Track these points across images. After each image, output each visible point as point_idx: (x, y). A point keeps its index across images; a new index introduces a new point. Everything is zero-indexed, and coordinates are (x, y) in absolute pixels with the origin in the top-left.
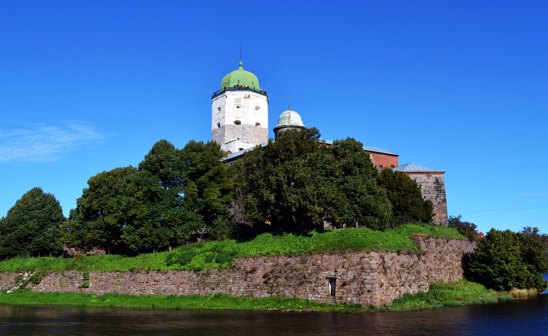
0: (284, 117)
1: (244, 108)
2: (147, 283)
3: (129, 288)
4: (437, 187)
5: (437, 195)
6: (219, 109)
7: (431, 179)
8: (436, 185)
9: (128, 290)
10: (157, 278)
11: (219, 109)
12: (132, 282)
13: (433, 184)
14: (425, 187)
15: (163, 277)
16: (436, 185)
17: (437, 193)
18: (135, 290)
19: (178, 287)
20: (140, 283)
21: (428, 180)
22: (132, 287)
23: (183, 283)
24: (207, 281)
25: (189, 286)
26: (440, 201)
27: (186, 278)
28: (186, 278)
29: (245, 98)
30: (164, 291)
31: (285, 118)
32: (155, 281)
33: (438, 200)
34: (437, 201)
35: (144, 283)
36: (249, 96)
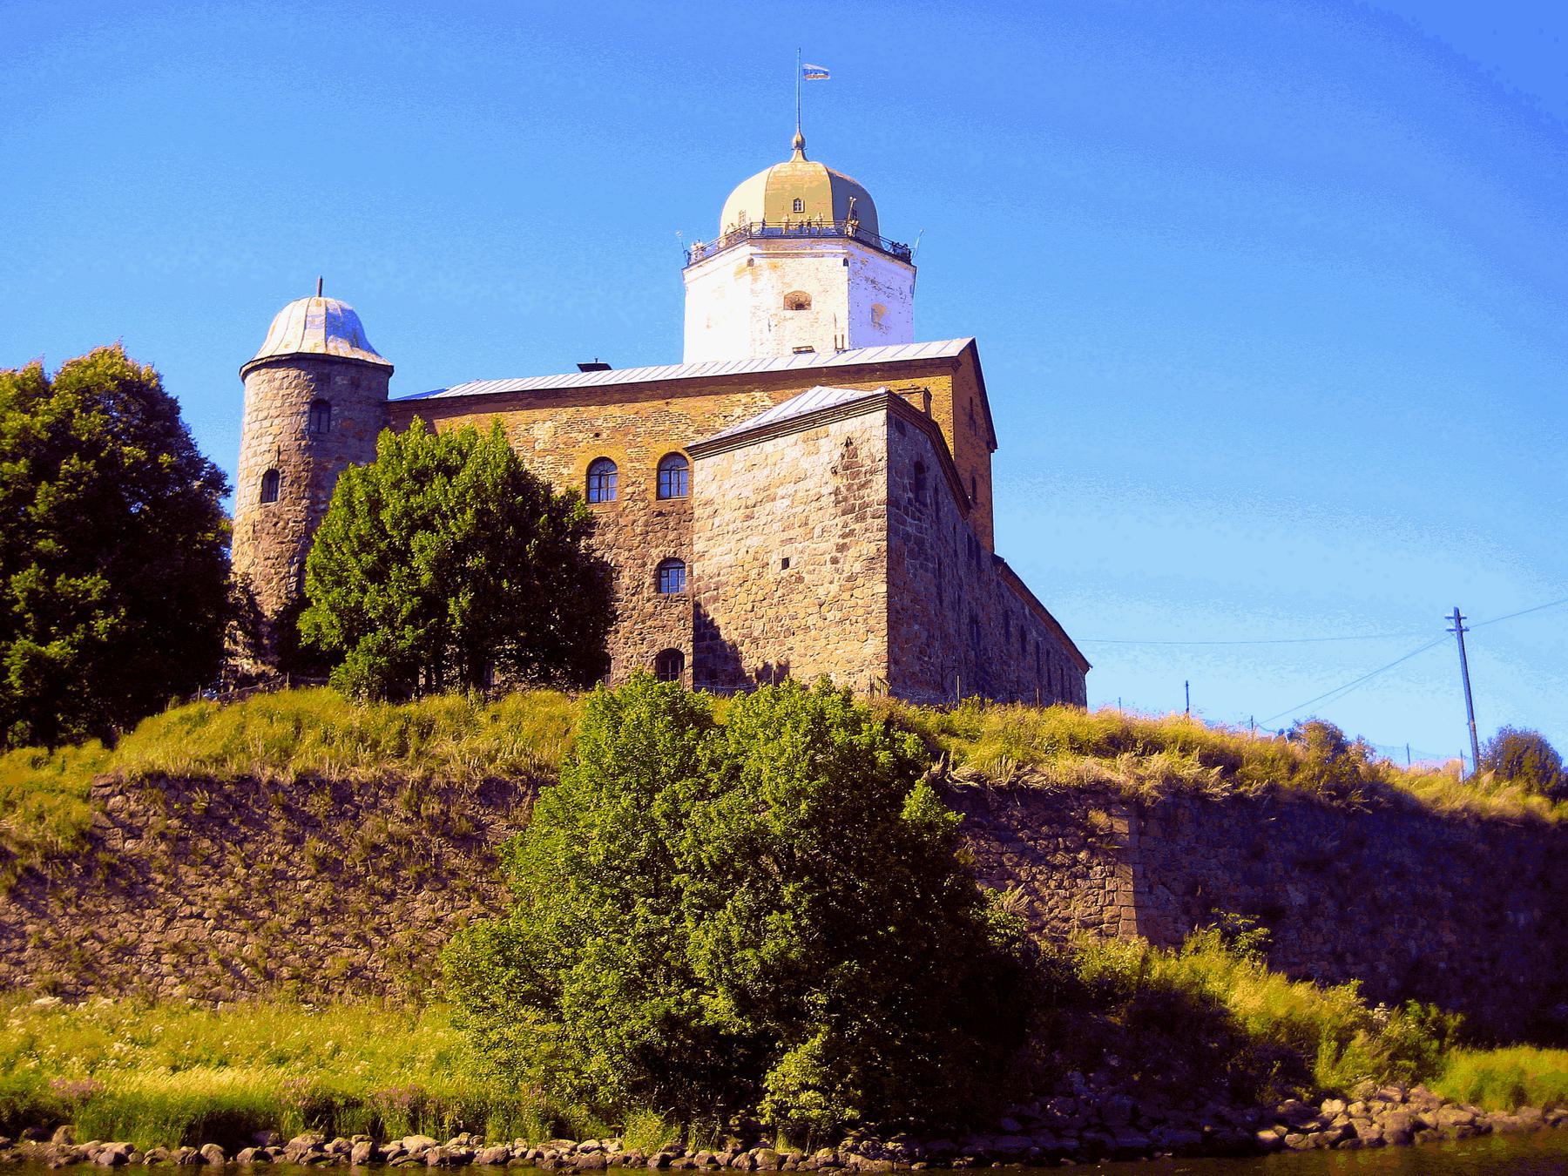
4: (849, 488)
5: (844, 536)
7: (823, 449)
8: (840, 482)
13: (828, 474)
14: (787, 502)
16: (840, 482)
17: (845, 525)
21: (805, 464)
26: (857, 567)
29: (739, 273)
33: (847, 568)
34: (837, 570)
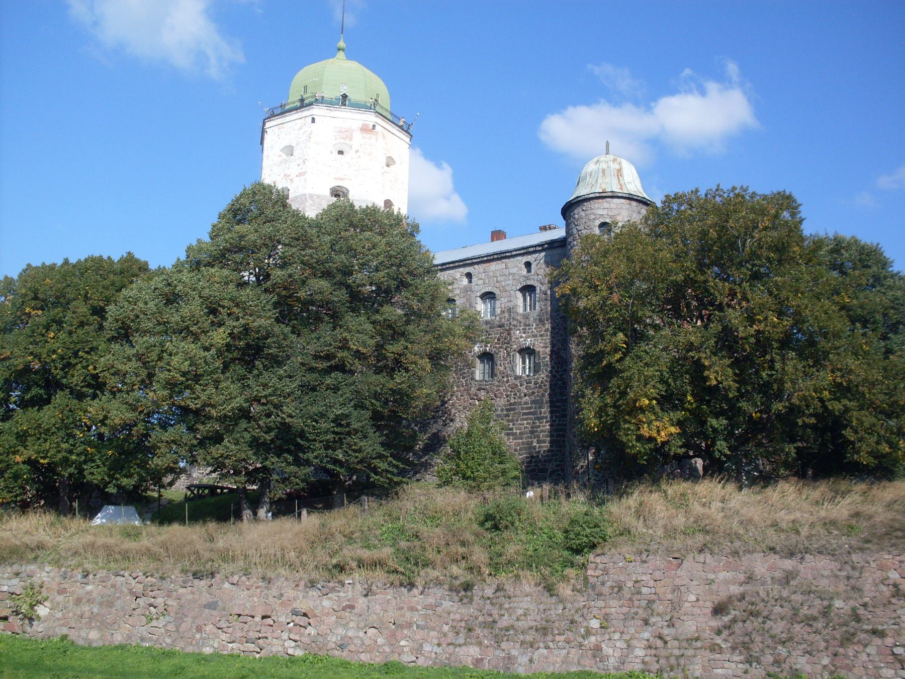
0: (603, 171)
1: (359, 157)
2: (264, 617)
3: (199, 629)
6: (289, 151)
9: (198, 636)
10: (302, 606)
11: (289, 151)
12: (207, 611)
15: (326, 603)
18: (224, 636)
19: (393, 638)
20: (239, 615)
22: (209, 628)
23: (409, 625)
24: (505, 622)
25: (433, 634)
27: (417, 610)
28: (417, 610)
30: (342, 647)
31: (607, 173)
32: (295, 613)
35: (253, 617)
36: (374, 126)
